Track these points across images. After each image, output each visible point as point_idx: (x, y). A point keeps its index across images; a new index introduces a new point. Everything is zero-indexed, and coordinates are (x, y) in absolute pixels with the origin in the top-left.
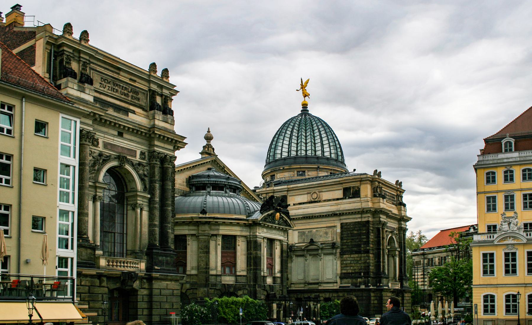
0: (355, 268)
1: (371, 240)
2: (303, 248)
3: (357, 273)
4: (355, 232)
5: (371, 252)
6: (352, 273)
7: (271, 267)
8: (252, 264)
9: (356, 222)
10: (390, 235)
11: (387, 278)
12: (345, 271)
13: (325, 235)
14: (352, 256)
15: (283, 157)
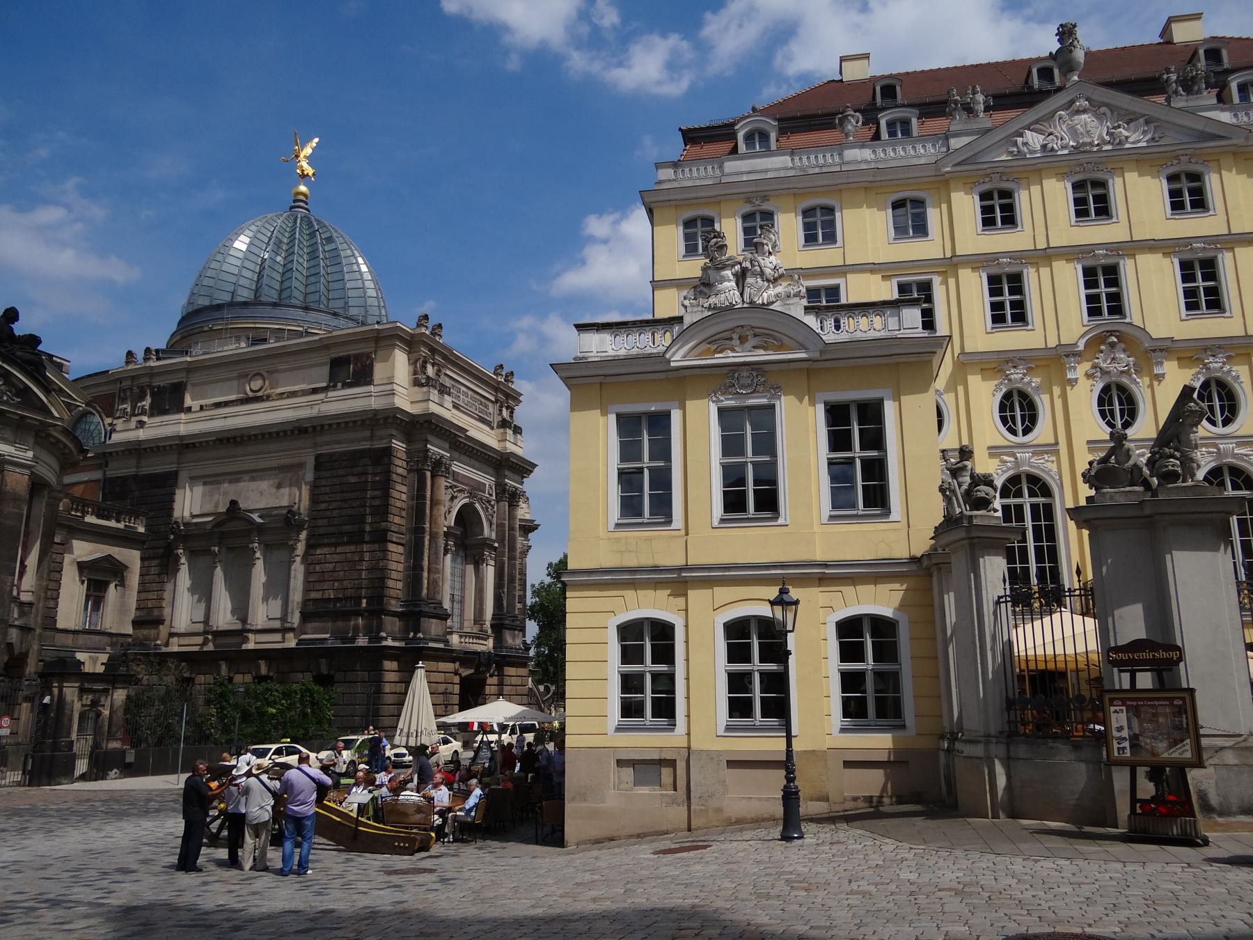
0: (346, 583)
2: (209, 527)
4: (353, 480)
6: (336, 600)
9: (356, 451)
13: (274, 490)
14: (339, 549)
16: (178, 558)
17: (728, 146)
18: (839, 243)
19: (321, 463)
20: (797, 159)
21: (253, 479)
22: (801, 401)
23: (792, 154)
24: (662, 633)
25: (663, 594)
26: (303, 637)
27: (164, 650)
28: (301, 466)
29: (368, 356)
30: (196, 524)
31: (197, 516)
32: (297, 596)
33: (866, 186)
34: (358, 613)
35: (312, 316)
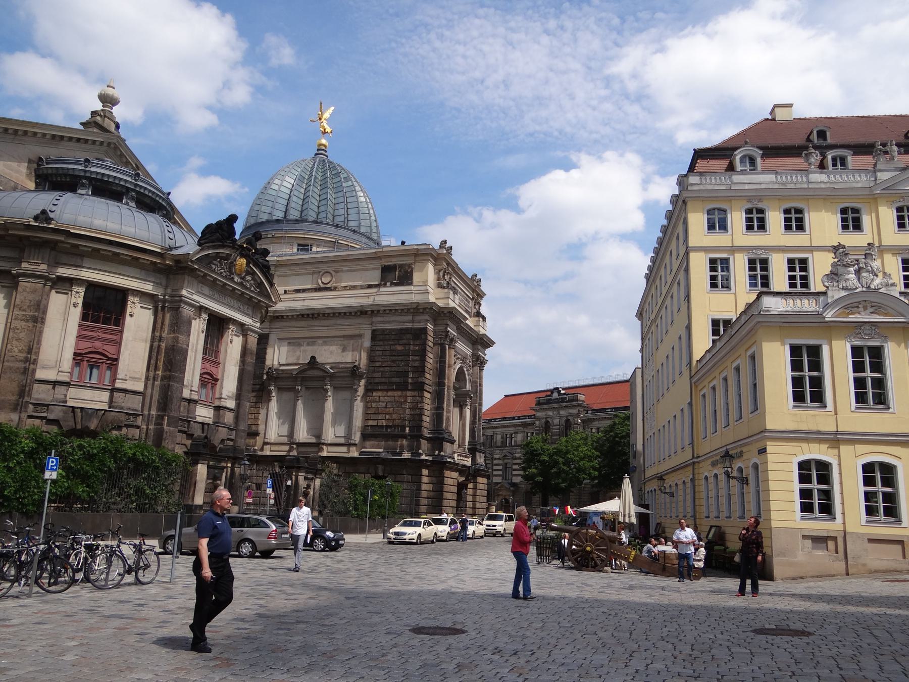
0: (394, 416)
1: (429, 366)
2: (294, 373)
3: (398, 426)
4: (399, 348)
5: (427, 388)
6: (387, 427)
7: (210, 380)
8: (161, 365)
9: (401, 329)
10: (458, 366)
11: (452, 442)
12: (375, 423)
15: (275, 218)
16: (270, 392)
17: (724, 163)
18: (808, 232)
19: (376, 336)
20: (779, 177)
21: (325, 343)
22: (899, 346)
23: (776, 173)
24: (824, 469)
25: (824, 447)
26: (363, 450)
27: (259, 453)
28: (360, 336)
29: (409, 266)
30: (283, 370)
31: (283, 365)
32: (358, 422)
33: (825, 197)
34: (404, 437)
35: (341, 232)
